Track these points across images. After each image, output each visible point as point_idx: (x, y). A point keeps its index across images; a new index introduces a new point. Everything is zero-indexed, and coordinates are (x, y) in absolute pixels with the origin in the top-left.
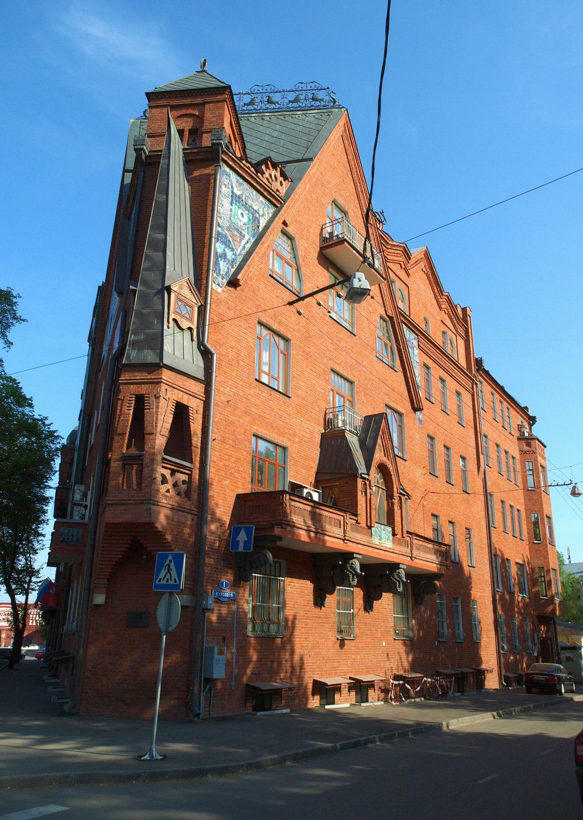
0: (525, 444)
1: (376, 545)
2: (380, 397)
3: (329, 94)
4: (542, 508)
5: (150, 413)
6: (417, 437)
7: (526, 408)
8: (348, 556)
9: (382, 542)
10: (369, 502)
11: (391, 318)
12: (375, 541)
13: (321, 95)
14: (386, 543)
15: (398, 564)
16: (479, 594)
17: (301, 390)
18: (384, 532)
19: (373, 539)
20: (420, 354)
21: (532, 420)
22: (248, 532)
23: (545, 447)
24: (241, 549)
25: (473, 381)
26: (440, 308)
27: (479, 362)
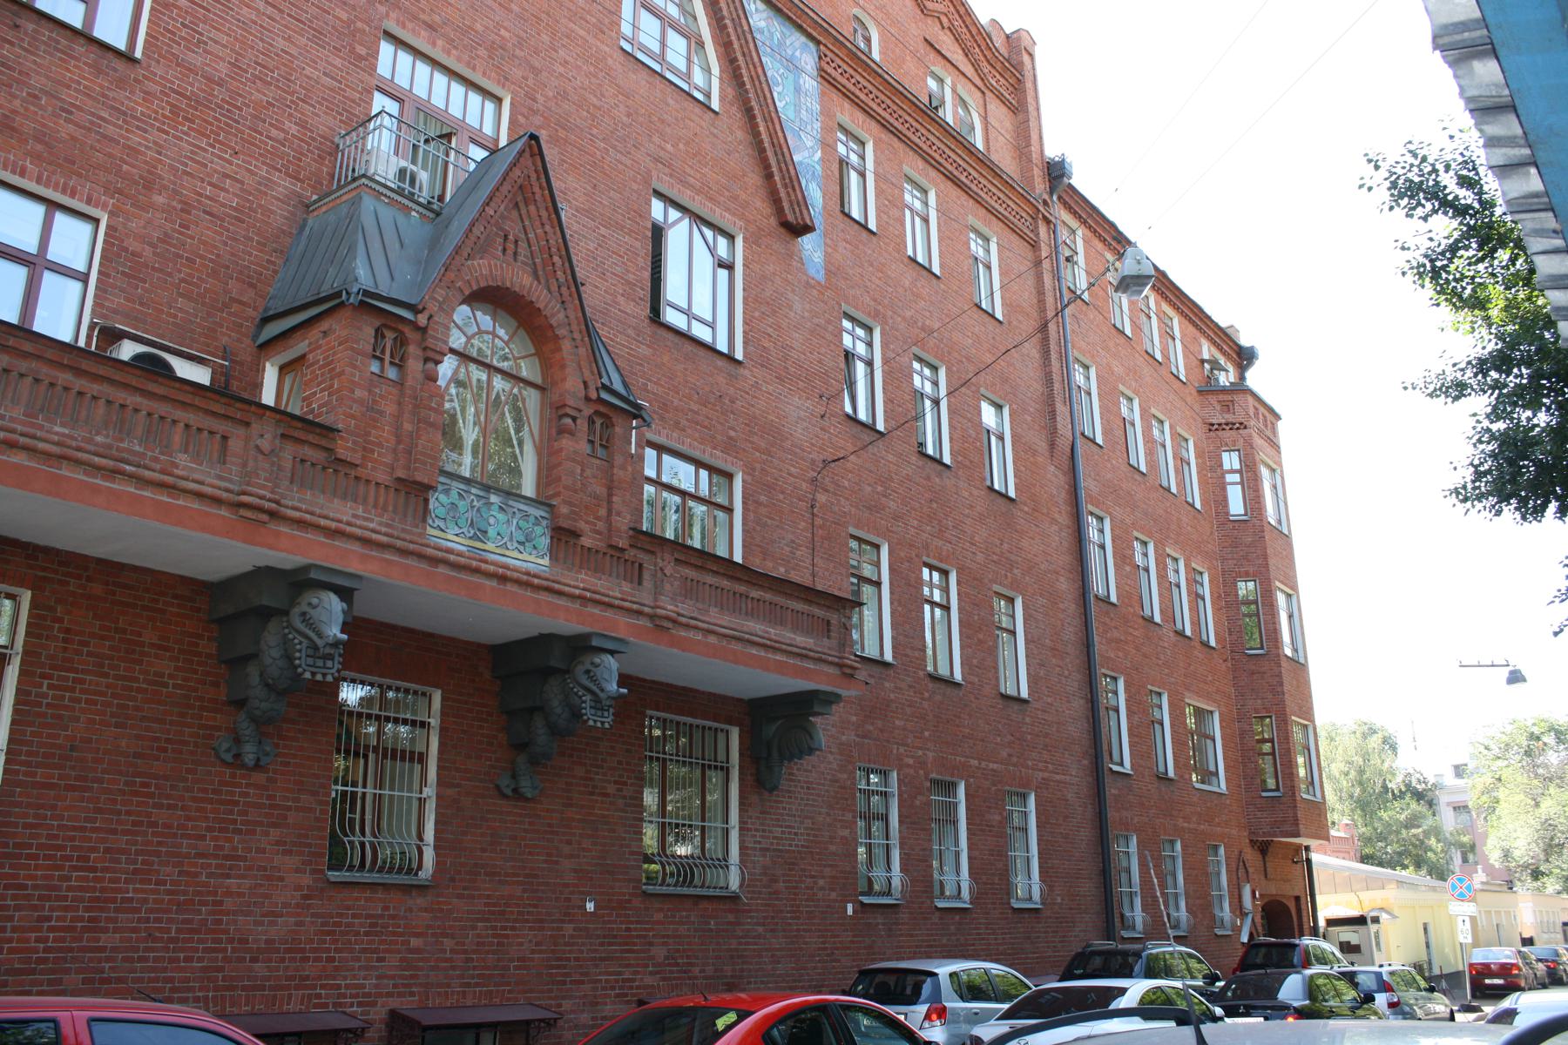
0: (1218, 407)
1: (460, 554)
2: (629, 162)
6: (797, 306)
9: (490, 546)
12: (451, 538)
14: (515, 554)
17: (205, 51)
18: (501, 516)
19: (430, 531)
20: (823, 94)
21: (1244, 357)
23: (1278, 417)
27: (1056, 172)
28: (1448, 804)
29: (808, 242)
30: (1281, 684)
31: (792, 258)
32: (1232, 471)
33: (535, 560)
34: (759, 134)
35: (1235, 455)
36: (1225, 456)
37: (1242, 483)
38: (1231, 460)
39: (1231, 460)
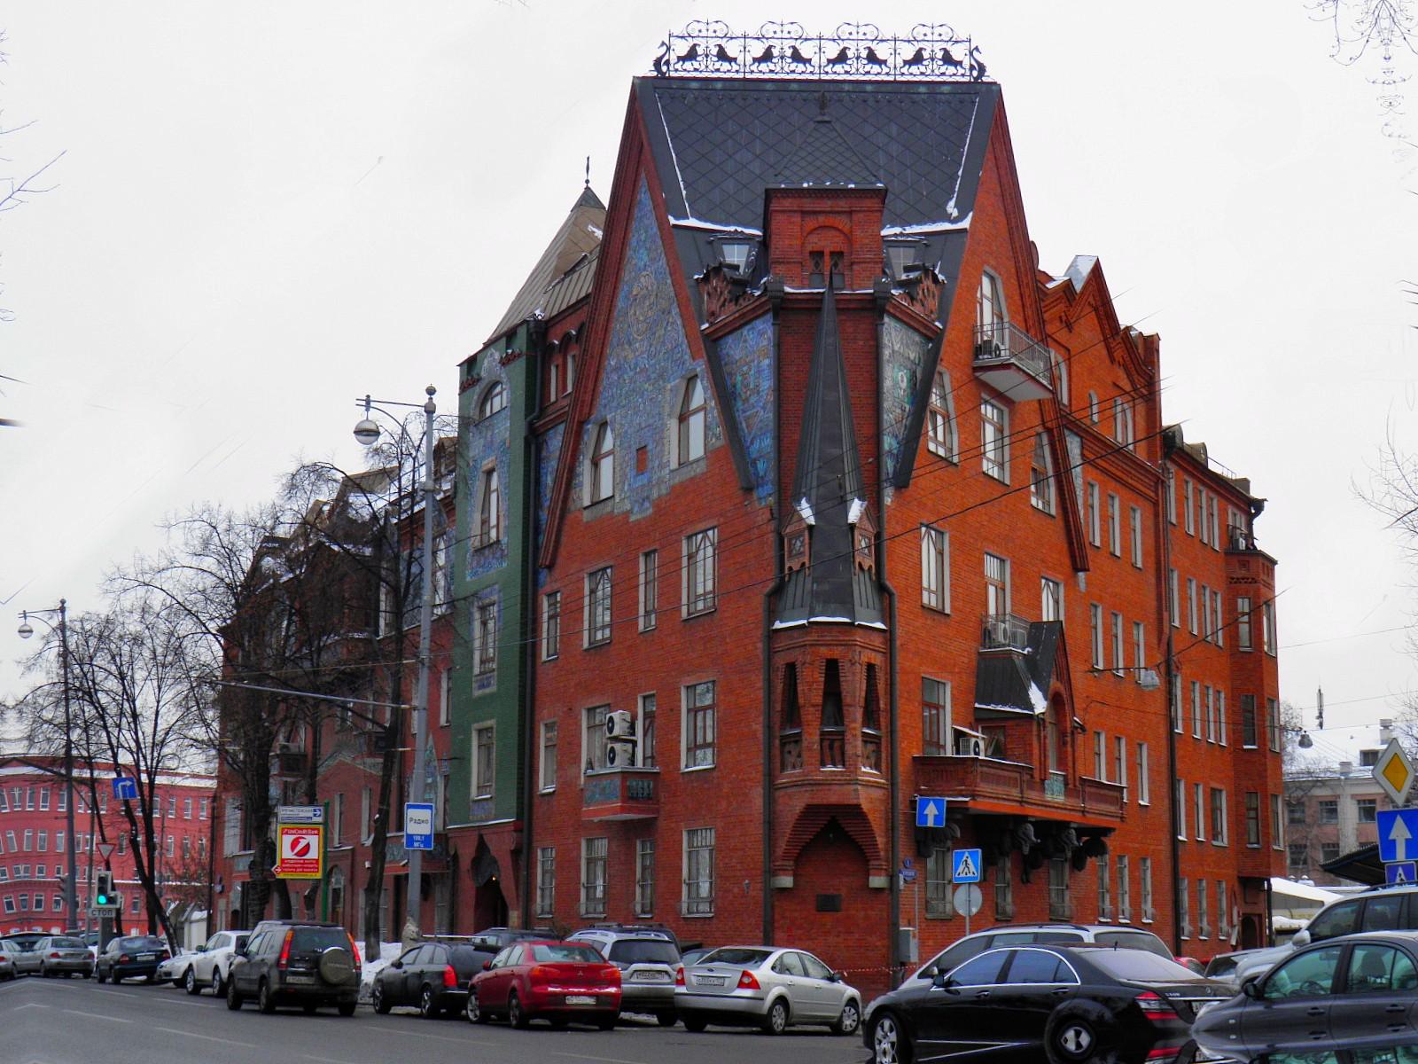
0: (1237, 565)
3: (971, 54)
4: (1262, 686)
5: (846, 681)
7: (1245, 483)
8: (1021, 819)
11: (1049, 431)
12: (1048, 797)
13: (958, 53)
15: (1069, 822)
16: (1152, 847)
21: (1253, 507)
22: (937, 804)
23: (1274, 562)
24: (930, 823)
26: (1112, 360)
28: (1353, 796)
29: (1081, 574)
30: (1266, 770)
31: (1077, 584)
32: (1243, 614)
33: (1060, 799)
34: (1069, 521)
35: (1246, 601)
36: (1240, 601)
37: (1249, 622)
38: (1243, 605)
39: (1243, 605)
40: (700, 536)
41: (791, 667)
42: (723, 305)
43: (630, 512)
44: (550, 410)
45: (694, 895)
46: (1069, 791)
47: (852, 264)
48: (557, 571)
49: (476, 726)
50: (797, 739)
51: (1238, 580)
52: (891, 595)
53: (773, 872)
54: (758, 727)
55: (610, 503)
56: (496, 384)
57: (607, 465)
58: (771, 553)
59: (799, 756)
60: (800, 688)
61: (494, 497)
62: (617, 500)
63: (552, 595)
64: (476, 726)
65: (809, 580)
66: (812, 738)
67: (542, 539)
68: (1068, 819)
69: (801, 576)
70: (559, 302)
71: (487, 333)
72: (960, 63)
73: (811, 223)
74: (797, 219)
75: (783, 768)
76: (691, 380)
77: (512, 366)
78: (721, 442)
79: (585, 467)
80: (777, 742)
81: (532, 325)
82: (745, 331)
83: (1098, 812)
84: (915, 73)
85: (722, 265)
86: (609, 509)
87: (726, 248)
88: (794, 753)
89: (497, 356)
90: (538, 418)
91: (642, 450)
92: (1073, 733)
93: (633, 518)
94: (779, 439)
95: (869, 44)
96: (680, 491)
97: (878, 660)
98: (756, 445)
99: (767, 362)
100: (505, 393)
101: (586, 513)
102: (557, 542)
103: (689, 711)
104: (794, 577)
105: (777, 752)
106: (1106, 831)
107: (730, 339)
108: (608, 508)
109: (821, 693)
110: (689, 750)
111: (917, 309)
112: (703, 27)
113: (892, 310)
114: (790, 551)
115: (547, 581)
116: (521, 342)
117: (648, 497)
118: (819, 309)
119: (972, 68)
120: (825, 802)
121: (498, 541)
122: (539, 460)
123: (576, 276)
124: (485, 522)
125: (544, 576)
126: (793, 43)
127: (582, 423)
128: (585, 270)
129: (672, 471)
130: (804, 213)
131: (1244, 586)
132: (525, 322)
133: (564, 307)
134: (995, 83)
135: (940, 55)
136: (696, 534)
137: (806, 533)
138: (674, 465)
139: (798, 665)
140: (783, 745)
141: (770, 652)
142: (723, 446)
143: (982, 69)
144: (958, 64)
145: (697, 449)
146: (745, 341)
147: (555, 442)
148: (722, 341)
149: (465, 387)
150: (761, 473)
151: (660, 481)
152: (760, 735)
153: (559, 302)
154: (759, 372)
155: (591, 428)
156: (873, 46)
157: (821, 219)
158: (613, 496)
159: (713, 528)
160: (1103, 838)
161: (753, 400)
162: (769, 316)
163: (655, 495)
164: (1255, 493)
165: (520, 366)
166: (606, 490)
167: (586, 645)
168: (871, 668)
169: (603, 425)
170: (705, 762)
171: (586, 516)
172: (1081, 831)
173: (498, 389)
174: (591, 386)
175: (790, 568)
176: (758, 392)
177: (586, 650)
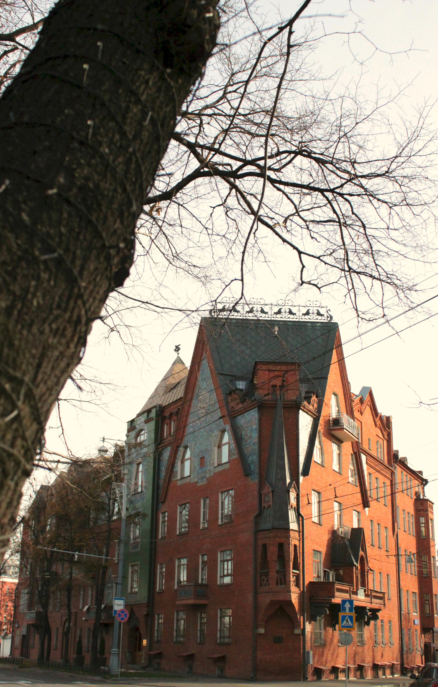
7: (421, 472)
10: (357, 577)
13: (322, 311)
21: (424, 482)
23: (433, 504)
25: (392, 471)
26: (376, 426)
32: (422, 523)
36: (421, 518)
39: (422, 520)
40: (226, 493)
41: (265, 546)
42: (237, 404)
43: (197, 482)
44: (164, 441)
45: (222, 635)
46: (366, 595)
47: (288, 390)
48: (167, 503)
49: (131, 564)
50: (267, 574)
51: (420, 510)
52: (302, 517)
53: (257, 627)
54: (251, 568)
55: (189, 478)
56: (142, 430)
57: (187, 464)
58: (256, 501)
59: (268, 581)
60: (268, 554)
61: (140, 474)
62: (192, 477)
63: (164, 513)
64: (131, 564)
65: (272, 512)
66: (273, 575)
67: (160, 491)
68: (365, 606)
69: (269, 510)
70: (169, 399)
71: (138, 411)
72: (323, 315)
73: (272, 375)
74: (267, 373)
75: (261, 585)
76: (223, 431)
77: (149, 424)
78: (236, 457)
79: (179, 463)
80: (259, 575)
81: (158, 408)
82: (246, 414)
83: (376, 604)
84: (306, 319)
85: (237, 389)
86: (188, 481)
87: (237, 383)
88: (265, 580)
89: (143, 420)
90: (159, 444)
91: (202, 459)
92: (367, 572)
93: (198, 485)
94: (260, 456)
95: (289, 307)
96: (217, 475)
97: (297, 544)
98: (250, 458)
99: (255, 427)
100: (146, 434)
101: (178, 482)
102: (166, 493)
103: (221, 561)
104: (266, 510)
105: (258, 579)
106: (378, 610)
107: (240, 417)
108: (188, 480)
109: (276, 556)
110: (221, 577)
111: (311, 407)
112: (228, 299)
113: (302, 408)
114: (264, 500)
115: (163, 508)
116: (153, 414)
117: (205, 477)
118: (275, 407)
119: (328, 317)
120: (278, 599)
121: (142, 492)
122: (159, 461)
123: (175, 390)
124: (136, 484)
125: (160, 505)
126: (261, 306)
127: (178, 447)
128: (180, 388)
129: (215, 467)
130: (269, 370)
131: (422, 512)
132: (155, 407)
133: (171, 402)
134: (336, 323)
135: (316, 312)
136: (224, 492)
137: (271, 494)
138: (216, 465)
139: (268, 545)
140: (261, 576)
141: (256, 539)
142: (236, 458)
143: (331, 318)
144: (322, 315)
145: (225, 458)
146: (246, 418)
147: (166, 454)
148: (238, 417)
149: (129, 431)
150: (252, 469)
151: (210, 471)
152: (252, 572)
153: (169, 399)
154: (252, 430)
155: (181, 449)
156: (291, 308)
157: (276, 373)
158: (190, 476)
159: (232, 490)
160: (377, 613)
161: (249, 441)
162: (257, 408)
163: (208, 476)
164: (425, 476)
165: (152, 424)
166: (187, 473)
167: (178, 533)
168: (295, 546)
169: (186, 447)
170: (227, 580)
171: (179, 483)
172: (370, 610)
173: (143, 432)
174: (181, 433)
175: (264, 507)
176: (251, 438)
177: (178, 535)
